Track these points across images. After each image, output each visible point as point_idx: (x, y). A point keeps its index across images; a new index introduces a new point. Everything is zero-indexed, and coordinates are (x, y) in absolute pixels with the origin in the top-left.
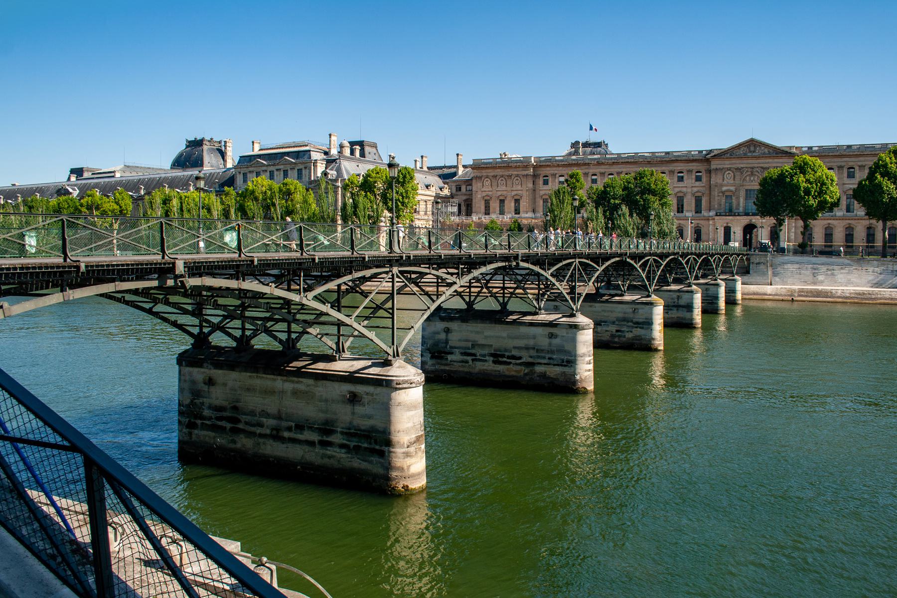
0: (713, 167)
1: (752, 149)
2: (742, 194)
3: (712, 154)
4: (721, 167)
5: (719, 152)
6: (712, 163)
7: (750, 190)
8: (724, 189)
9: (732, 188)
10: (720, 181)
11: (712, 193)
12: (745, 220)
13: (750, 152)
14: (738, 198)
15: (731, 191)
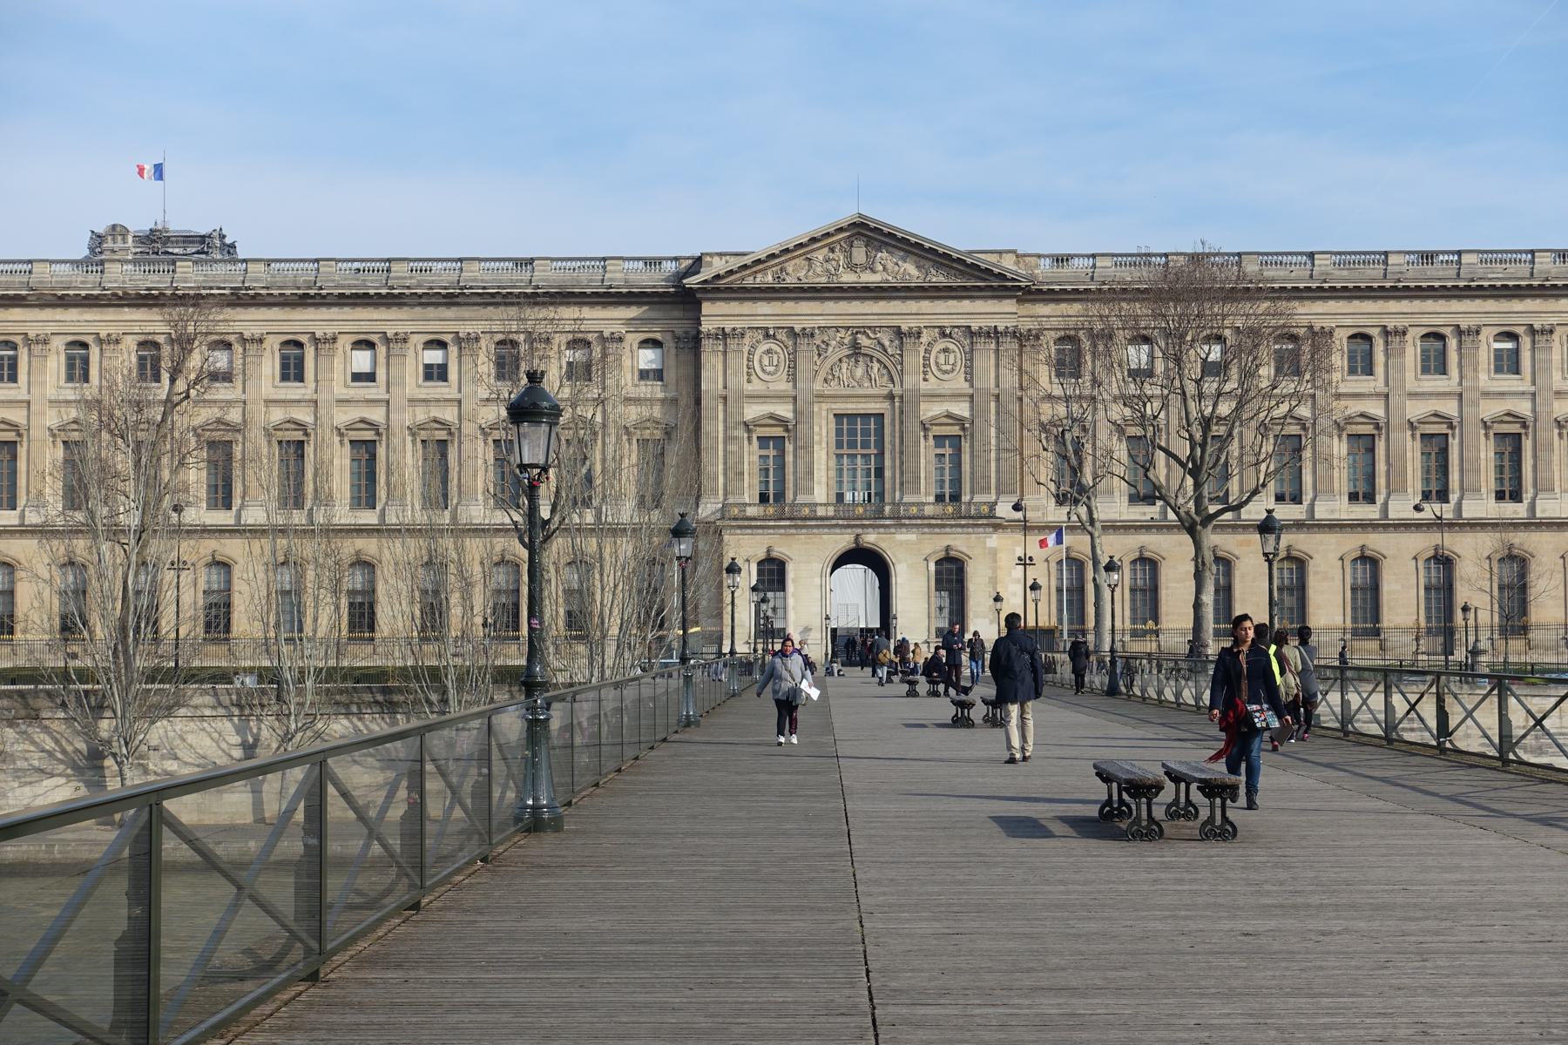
0: (707, 326)
1: (859, 254)
2: (823, 431)
3: (705, 274)
4: (739, 324)
5: (735, 263)
6: (707, 308)
7: (852, 417)
8: (752, 411)
9: (785, 411)
10: (738, 381)
11: (706, 426)
12: (843, 541)
13: (852, 267)
14: (809, 448)
15: (781, 422)
